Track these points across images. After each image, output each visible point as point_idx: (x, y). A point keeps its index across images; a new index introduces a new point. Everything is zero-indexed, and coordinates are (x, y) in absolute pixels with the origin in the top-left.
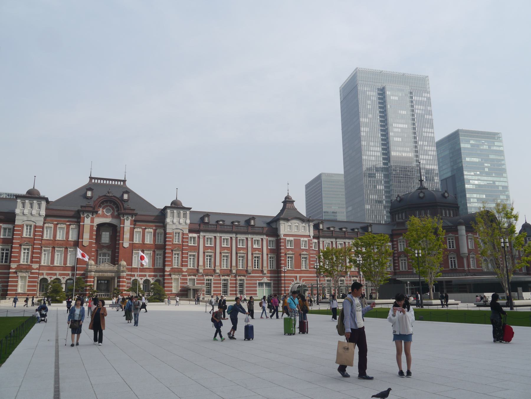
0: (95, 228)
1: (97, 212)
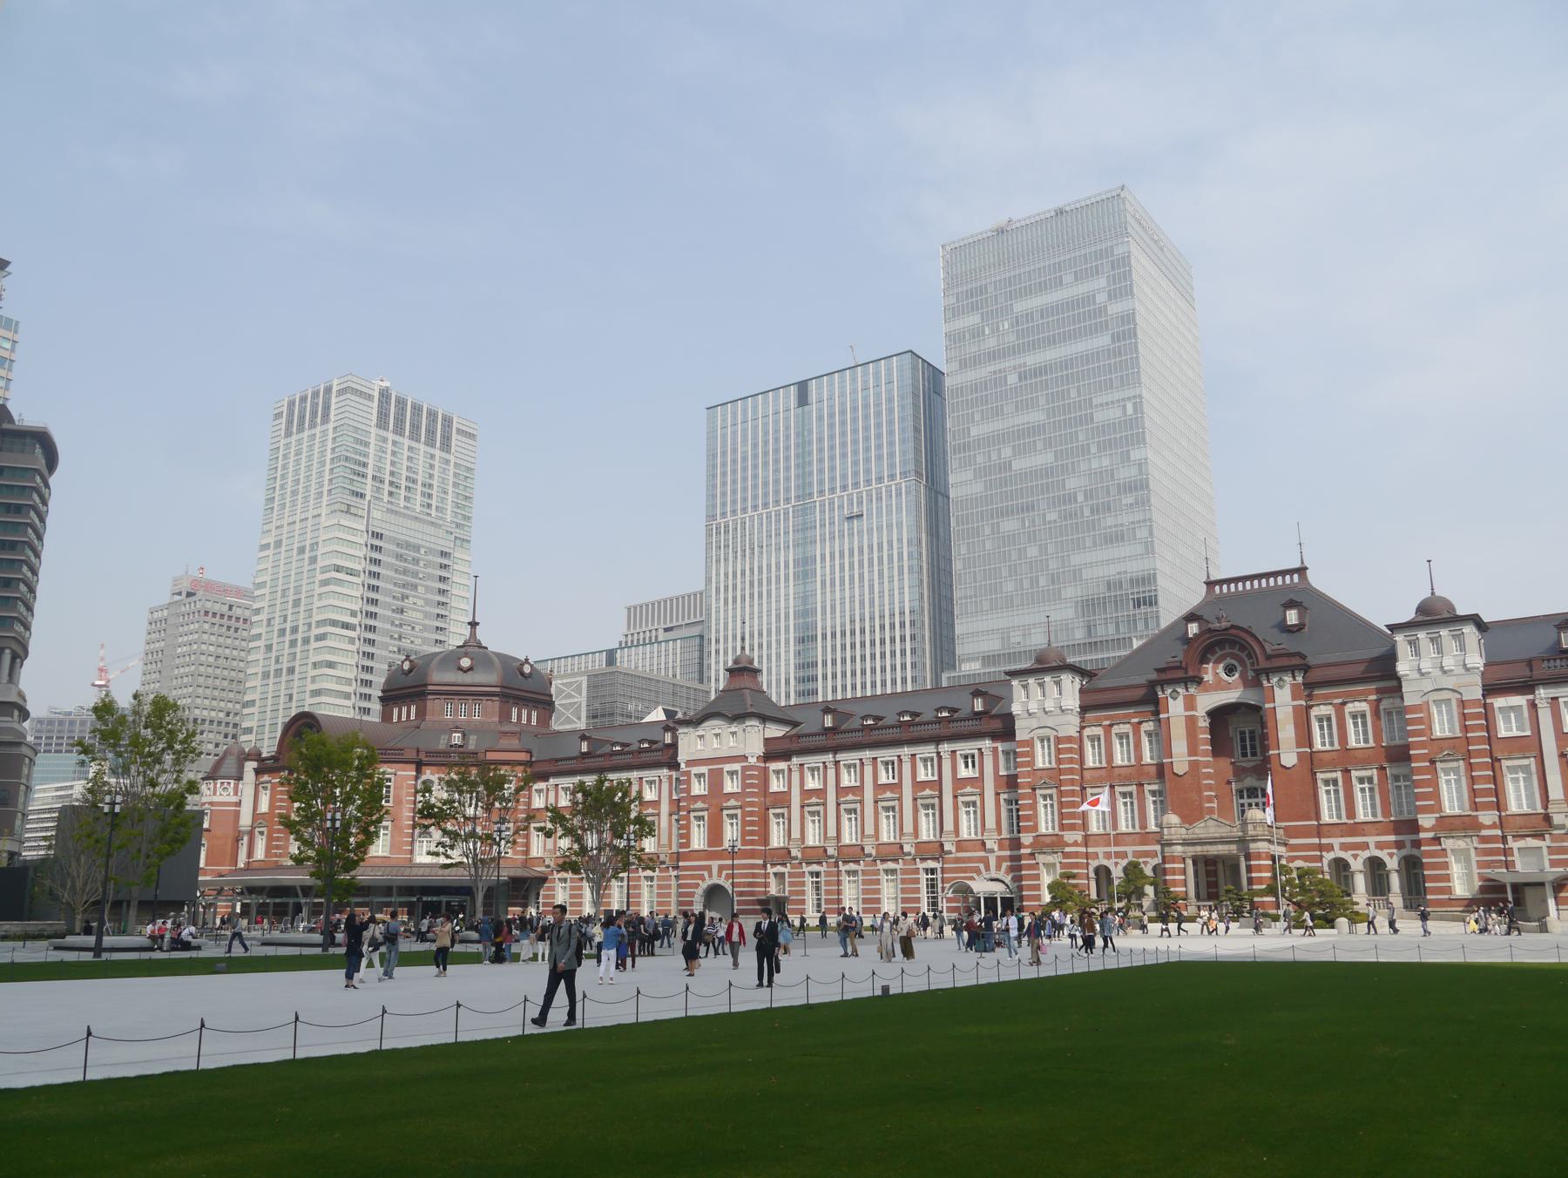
0: (1204, 723)
1: (1198, 681)
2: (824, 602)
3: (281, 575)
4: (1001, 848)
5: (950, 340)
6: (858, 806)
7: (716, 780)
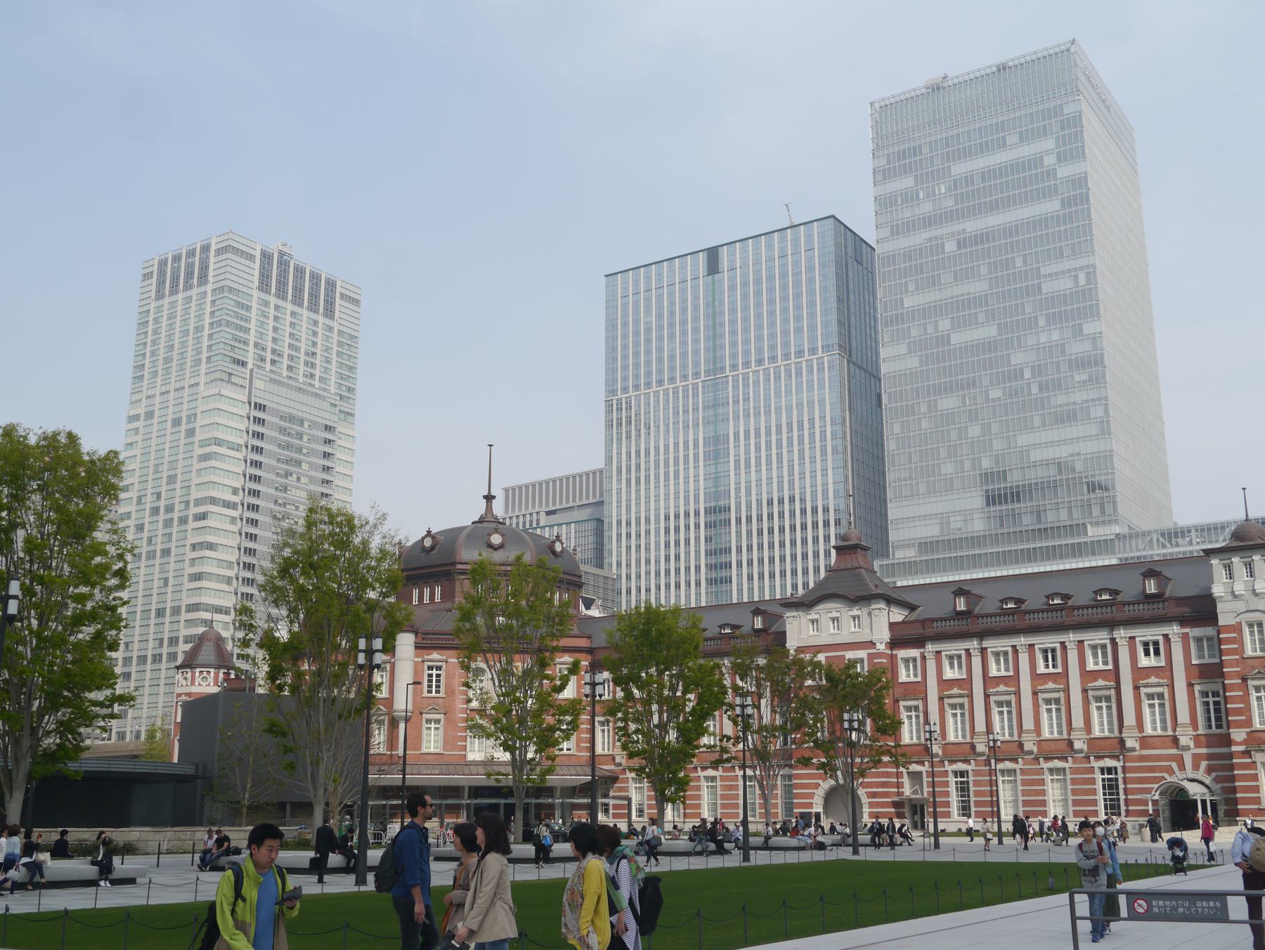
2: (738, 483)
3: (153, 449)
4: (1197, 745)
5: (880, 206)
6: (965, 701)
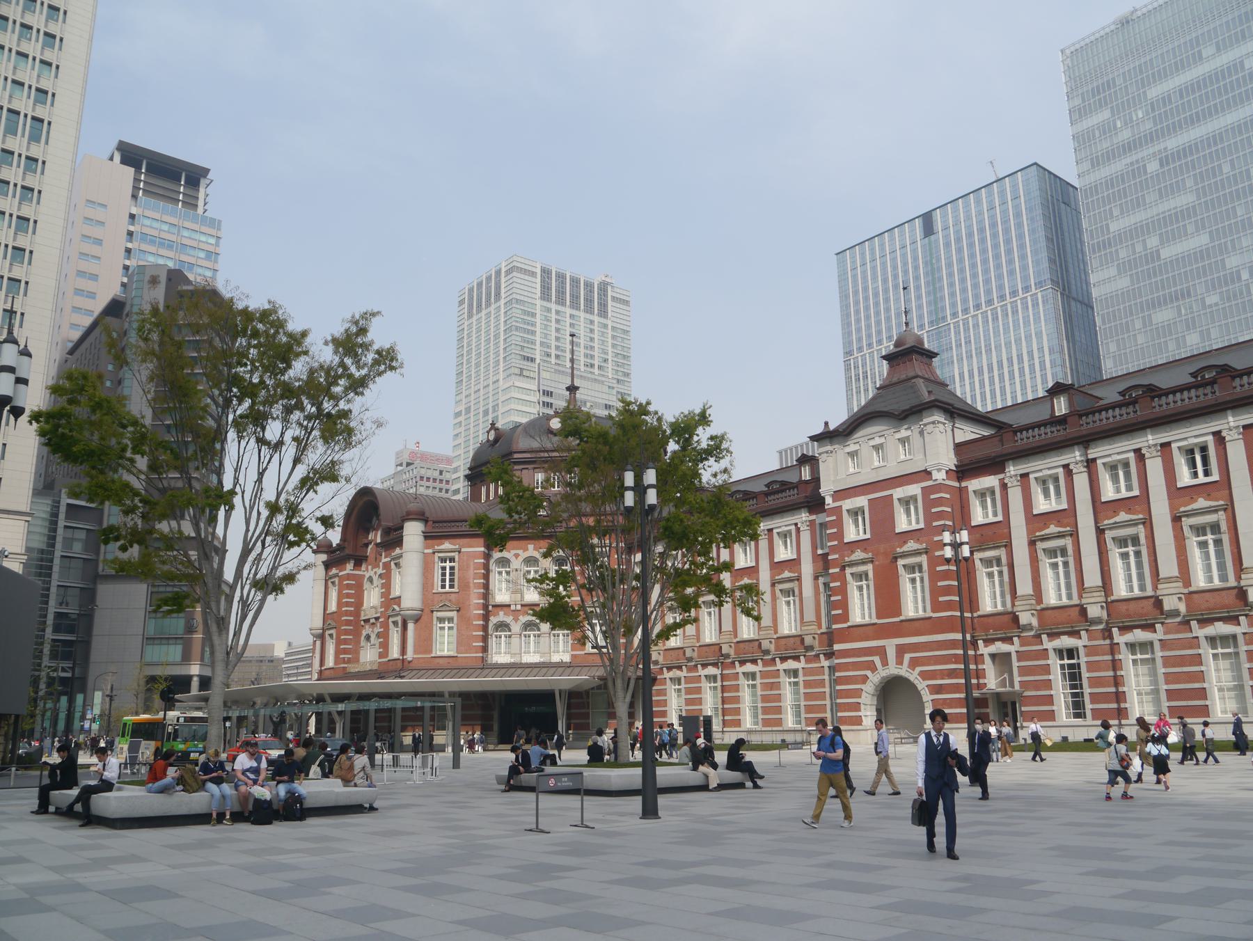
5: (1078, 142)
7: (882, 514)
